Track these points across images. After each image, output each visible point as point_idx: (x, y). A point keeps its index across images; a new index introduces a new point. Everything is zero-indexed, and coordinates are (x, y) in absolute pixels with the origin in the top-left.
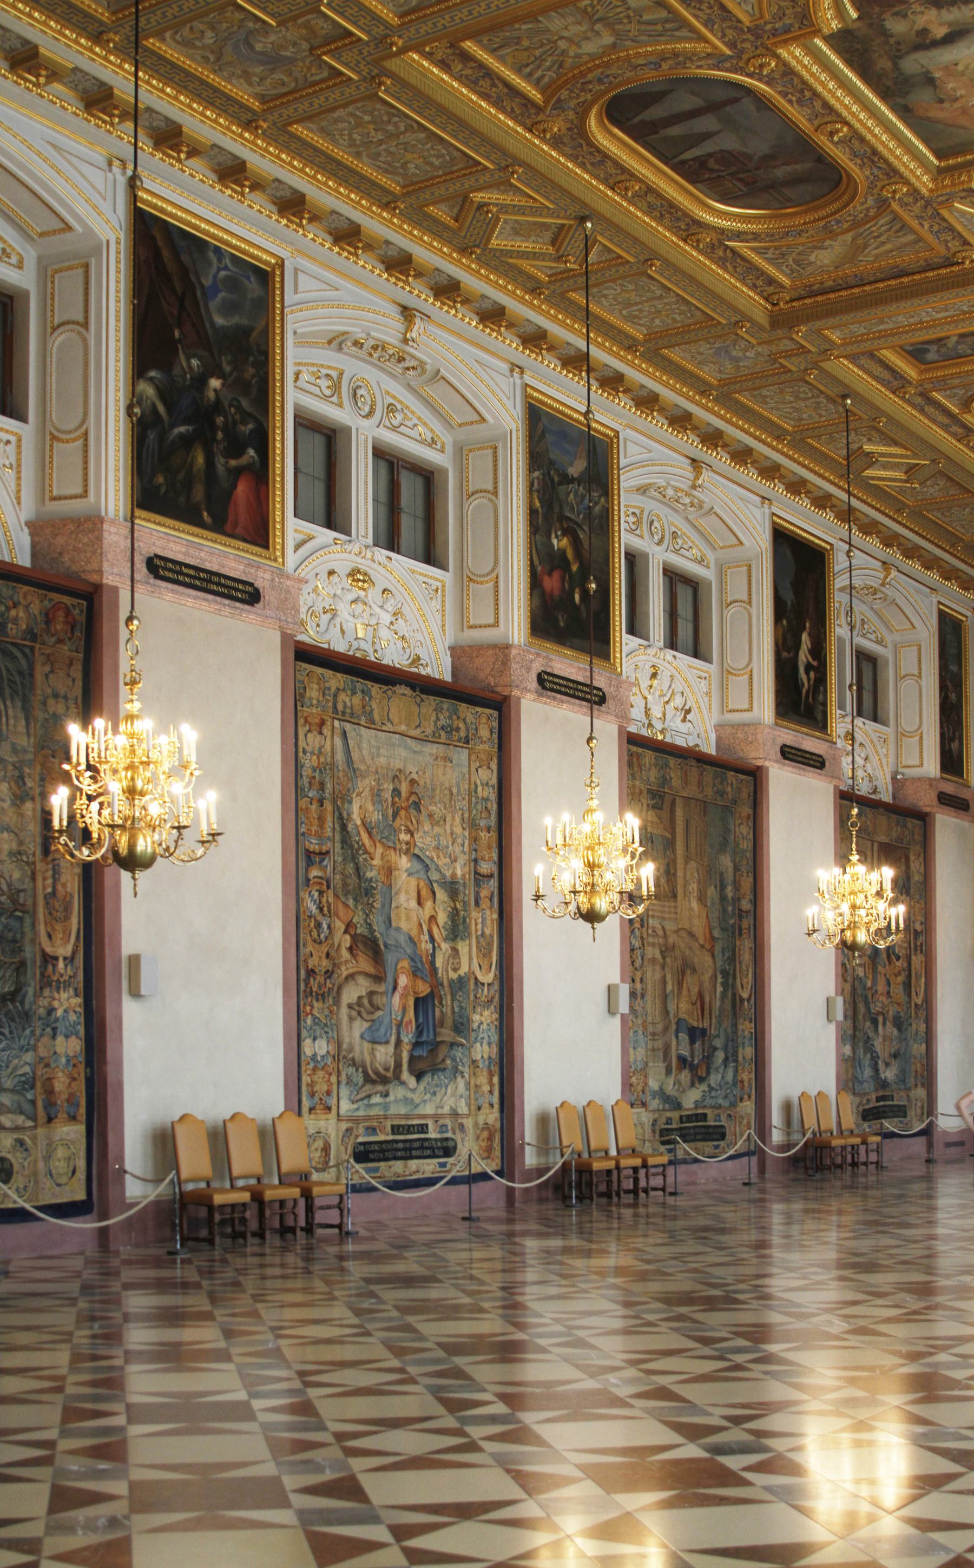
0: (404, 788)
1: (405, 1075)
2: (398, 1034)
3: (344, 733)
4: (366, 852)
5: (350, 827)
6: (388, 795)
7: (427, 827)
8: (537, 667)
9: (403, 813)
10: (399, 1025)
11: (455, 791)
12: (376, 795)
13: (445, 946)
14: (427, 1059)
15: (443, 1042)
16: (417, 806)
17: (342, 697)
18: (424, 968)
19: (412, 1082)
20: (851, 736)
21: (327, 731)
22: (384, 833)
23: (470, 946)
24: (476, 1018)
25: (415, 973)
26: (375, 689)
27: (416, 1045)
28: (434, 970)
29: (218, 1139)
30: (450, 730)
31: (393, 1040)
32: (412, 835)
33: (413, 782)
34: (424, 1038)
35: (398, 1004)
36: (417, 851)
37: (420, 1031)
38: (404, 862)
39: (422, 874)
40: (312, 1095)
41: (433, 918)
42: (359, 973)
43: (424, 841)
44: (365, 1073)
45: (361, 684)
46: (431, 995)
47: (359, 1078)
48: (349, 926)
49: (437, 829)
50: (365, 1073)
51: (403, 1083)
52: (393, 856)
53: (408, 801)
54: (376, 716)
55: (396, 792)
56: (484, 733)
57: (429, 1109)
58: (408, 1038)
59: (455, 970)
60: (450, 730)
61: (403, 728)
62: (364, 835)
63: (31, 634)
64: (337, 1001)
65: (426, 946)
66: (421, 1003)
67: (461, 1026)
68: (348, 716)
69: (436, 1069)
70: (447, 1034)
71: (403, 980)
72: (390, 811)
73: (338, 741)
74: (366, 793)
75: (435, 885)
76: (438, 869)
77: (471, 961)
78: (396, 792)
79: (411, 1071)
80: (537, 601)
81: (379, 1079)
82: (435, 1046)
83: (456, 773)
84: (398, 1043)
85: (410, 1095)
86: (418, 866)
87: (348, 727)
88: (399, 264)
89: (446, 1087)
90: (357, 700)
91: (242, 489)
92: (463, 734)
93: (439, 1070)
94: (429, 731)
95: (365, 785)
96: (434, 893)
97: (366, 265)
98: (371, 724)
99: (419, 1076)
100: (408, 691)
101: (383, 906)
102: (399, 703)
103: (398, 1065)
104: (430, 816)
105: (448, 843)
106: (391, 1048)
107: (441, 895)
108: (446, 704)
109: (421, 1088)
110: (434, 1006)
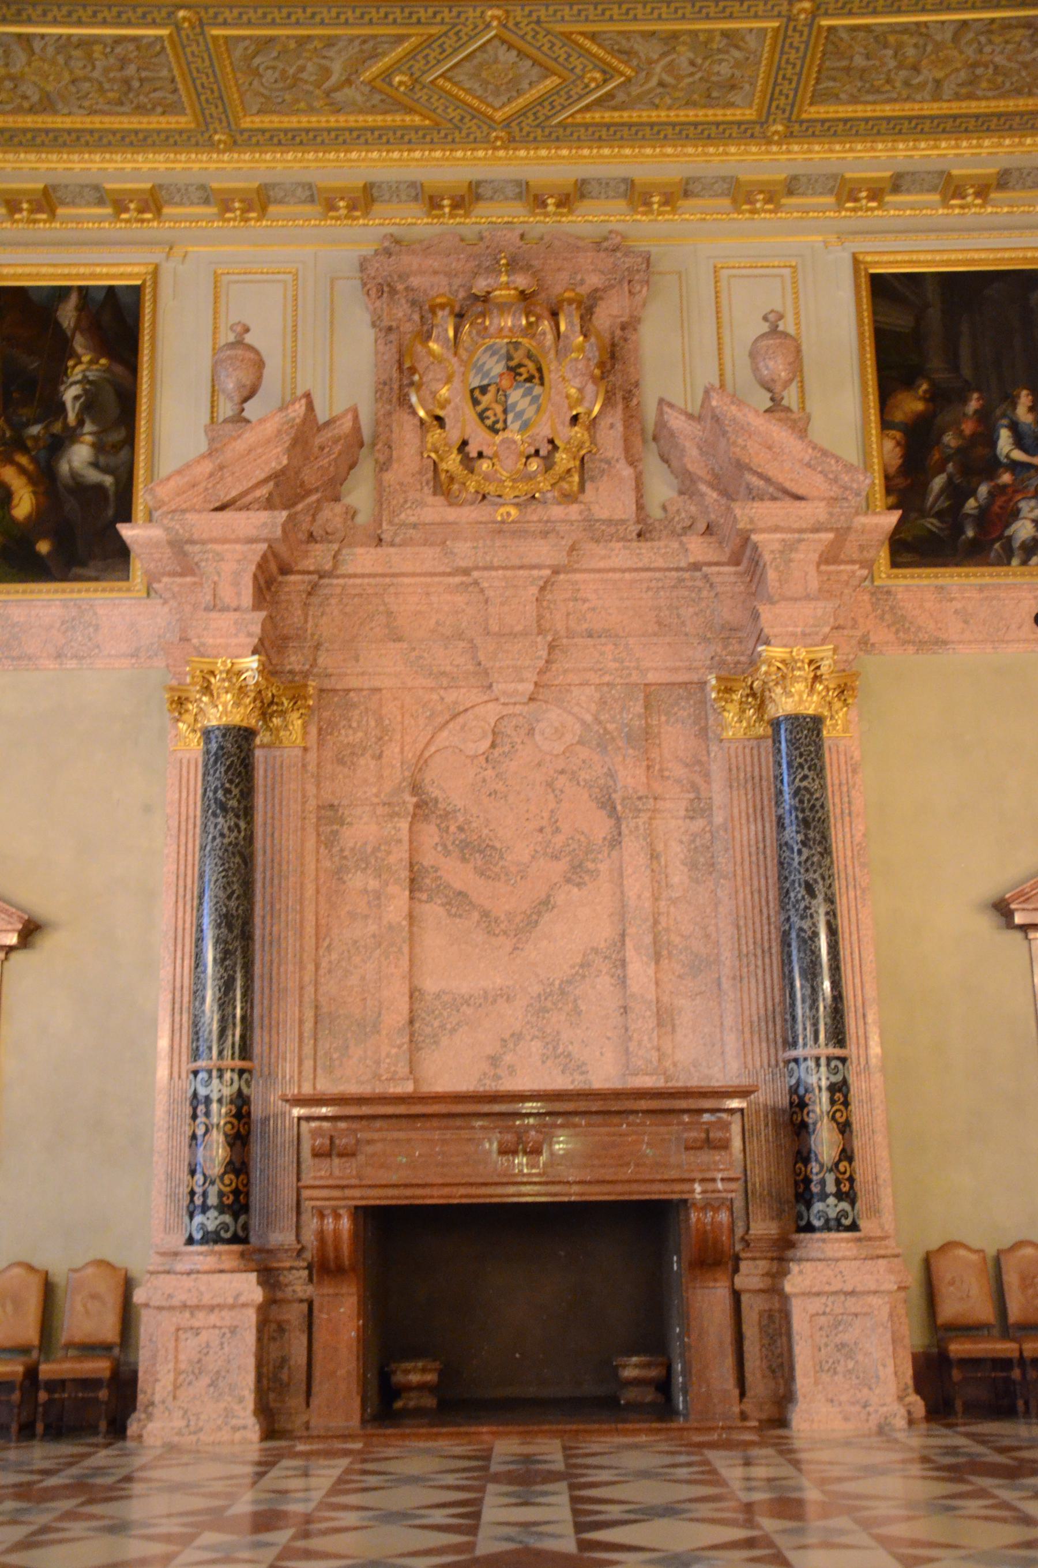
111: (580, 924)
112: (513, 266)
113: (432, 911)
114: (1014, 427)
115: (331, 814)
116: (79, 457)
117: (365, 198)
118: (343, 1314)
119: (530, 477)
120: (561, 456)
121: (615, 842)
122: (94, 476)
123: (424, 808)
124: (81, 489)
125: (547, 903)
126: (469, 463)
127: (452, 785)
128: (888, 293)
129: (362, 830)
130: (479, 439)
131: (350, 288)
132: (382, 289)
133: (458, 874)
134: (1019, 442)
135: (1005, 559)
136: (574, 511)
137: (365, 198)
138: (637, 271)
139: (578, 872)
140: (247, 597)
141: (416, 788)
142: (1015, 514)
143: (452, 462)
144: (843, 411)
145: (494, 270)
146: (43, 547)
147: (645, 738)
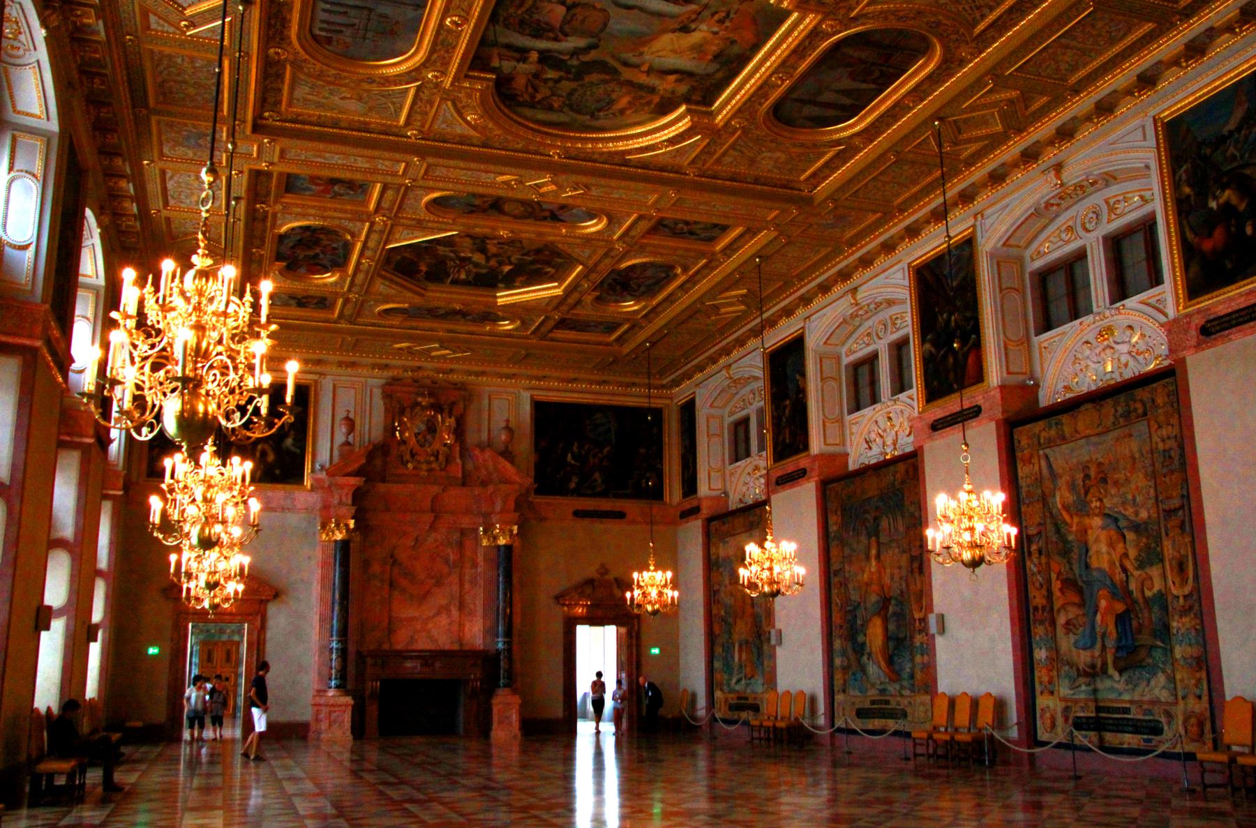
0: (1092, 473)
1: (1111, 671)
2: (1103, 641)
3: (1047, 457)
4: (1067, 524)
5: (1054, 511)
6: (1080, 482)
7: (1113, 491)
8: (1198, 321)
9: (1092, 490)
10: (1104, 635)
11: (1137, 455)
12: (1072, 487)
13: (1136, 573)
14: (1130, 658)
15: (1143, 646)
16: (1104, 480)
17: (1043, 434)
18: (1121, 592)
19: (1116, 675)
20: (757, 468)
21: (1035, 460)
22: (1081, 508)
23: (1164, 568)
24: (1175, 624)
25: (1114, 596)
26: (1065, 418)
27: (1118, 648)
28: (1130, 593)
29: (975, 703)
30: (1127, 415)
31: (1098, 646)
32: (1101, 500)
33: (1100, 464)
34: (1124, 642)
35: (1105, 622)
36: (1107, 511)
37: (1119, 639)
38: (1097, 521)
39: (1113, 526)
40: (1041, 683)
41: (1126, 555)
42: (1068, 604)
44: (1078, 670)
45: (1053, 420)
46: (1127, 611)
47: (1074, 673)
48: (1059, 574)
49: (1122, 490)
50: (1078, 670)
51: (1111, 677)
52: (1087, 521)
54: (1067, 434)
55: (1087, 477)
57: (1126, 697)
58: (1111, 643)
59: (1150, 589)
61: (1088, 432)
62: (1064, 513)
63: (903, 482)
64: (1053, 623)
65: (1119, 576)
66: (1122, 620)
67: (1164, 632)
68: (1050, 443)
69: (1139, 665)
70: (1145, 639)
71: (1103, 603)
72: (1082, 492)
73: (1043, 463)
74: (1064, 487)
75: (1126, 532)
76: (1126, 517)
77: (1157, 580)
78: (1087, 477)
79: (1116, 668)
80: (1194, 268)
81: (1093, 673)
82: (1134, 650)
83: (1132, 444)
84: (1104, 648)
85: (1116, 686)
86: (1109, 521)
87: (1048, 451)
88: (1030, 156)
89: (1149, 681)
90: (1053, 432)
91: (970, 360)
92: (1140, 411)
93: (1140, 666)
94: (1109, 423)
95: (1062, 482)
96: (1124, 536)
97: (1018, 176)
98: (1064, 439)
99: (1121, 672)
100: (1089, 406)
101: (1080, 556)
103: (1104, 664)
104: (1116, 483)
105: (1136, 496)
106: (1097, 653)
107: (1130, 536)
108: (1122, 398)
109: (1125, 676)
110: (1130, 619)
111: (439, 598)
112: (431, 395)
113: (396, 593)
114: (573, 453)
115: (366, 564)
116: (289, 442)
117: (386, 367)
118: (373, 711)
119: (429, 463)
120: (441, 457)
121: (450, 574)
122: (293, 449)
123: (395, 562)
124: (288, 452)
125: (428, 593)
126: (413, 455)
127: (402, 556)
128: (540, 408)
129: (376, 568)
130: (417, 448)
131: (378, 393)
132: (387, 396)
133: (404, 583)
134: (573, 458)
135: (566, 495)
136: (443, 473)
137: (387, 366)
138: (466, 393)
139: (439, 583)
140: (350, 502)
141: (392, 556)
142: (570, 481)
143: (408, 457)
144: (524, 446)
145: (423, 395)
146: (277, 472)
147: (461, 544)
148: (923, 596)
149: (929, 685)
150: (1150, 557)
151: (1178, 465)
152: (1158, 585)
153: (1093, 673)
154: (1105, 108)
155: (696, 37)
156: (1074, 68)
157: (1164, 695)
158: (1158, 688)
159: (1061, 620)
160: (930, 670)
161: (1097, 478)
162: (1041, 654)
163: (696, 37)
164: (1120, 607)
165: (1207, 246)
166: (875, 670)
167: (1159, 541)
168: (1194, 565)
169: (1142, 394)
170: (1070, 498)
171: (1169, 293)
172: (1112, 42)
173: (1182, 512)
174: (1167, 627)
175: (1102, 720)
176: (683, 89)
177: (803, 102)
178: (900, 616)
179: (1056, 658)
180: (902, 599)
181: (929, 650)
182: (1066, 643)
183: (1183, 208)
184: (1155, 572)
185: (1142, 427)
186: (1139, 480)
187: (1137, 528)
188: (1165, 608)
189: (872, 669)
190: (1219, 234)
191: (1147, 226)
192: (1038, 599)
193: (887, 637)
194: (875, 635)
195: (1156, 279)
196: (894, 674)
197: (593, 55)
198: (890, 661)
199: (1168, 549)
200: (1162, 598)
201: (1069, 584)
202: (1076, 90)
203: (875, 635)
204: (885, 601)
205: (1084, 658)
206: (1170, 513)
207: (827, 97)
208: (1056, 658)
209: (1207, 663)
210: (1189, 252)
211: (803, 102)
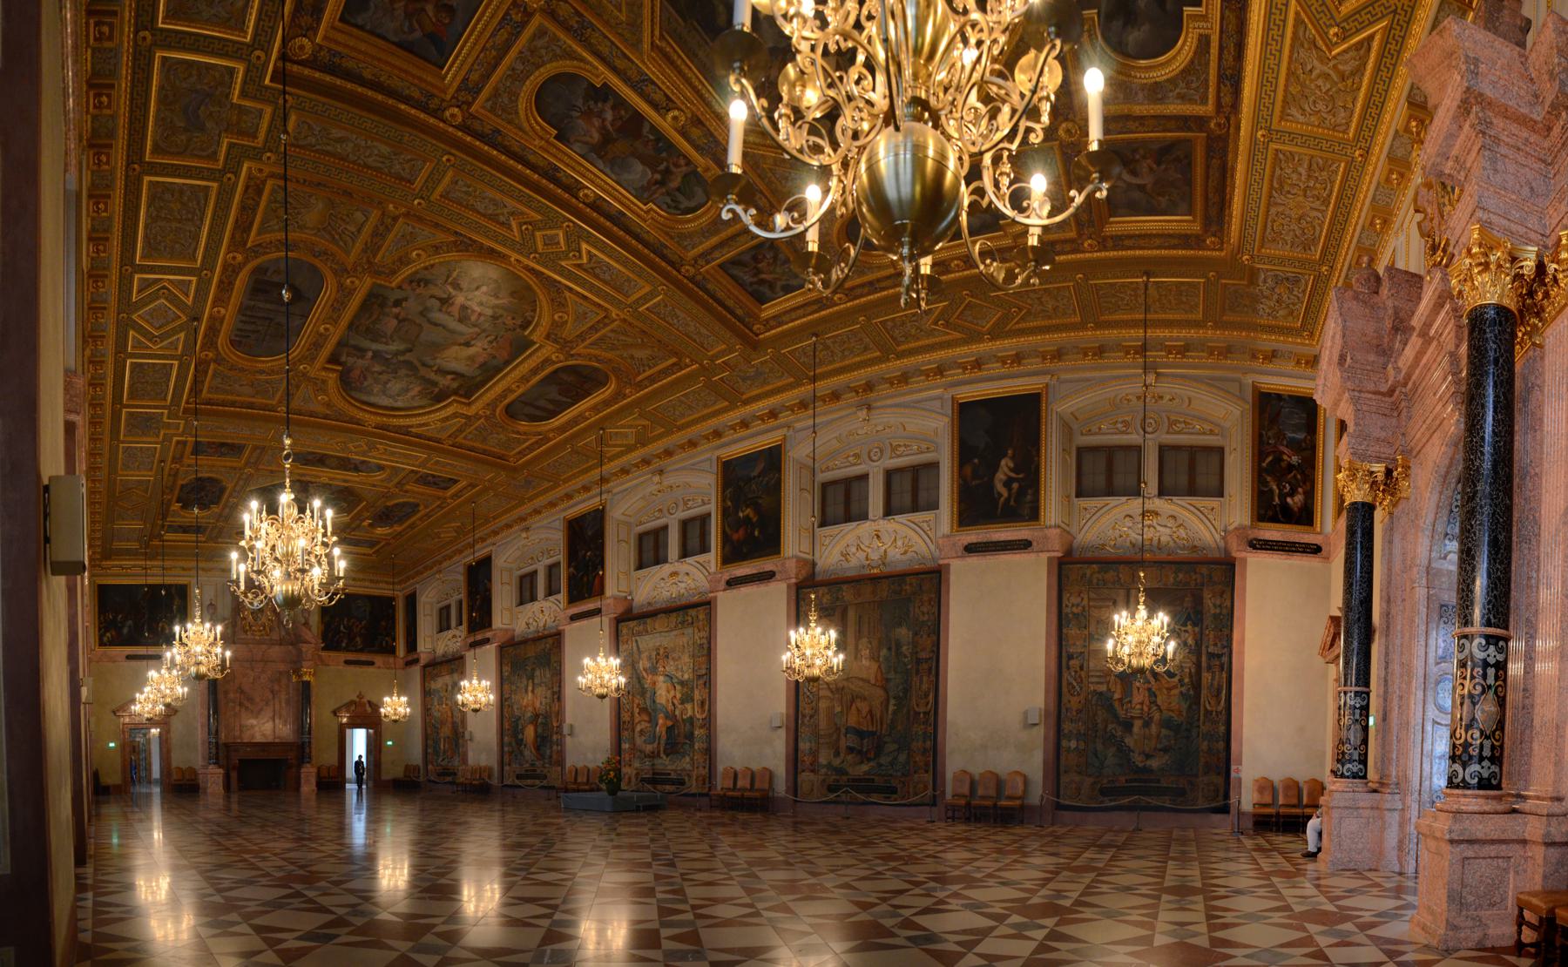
12: (650, 658)
22: (653, 670)
25: (667, 717)
30: (683, 623)
38: (661, 678)
43: (670, 669)
53: (663, 655)
56: (701, 616)
60: (683, 623)
65: (670, 707)
66: (670, 729)
67: (690, 736)
77: (689, 710)
95: (644, 655)
102: (659, 623)
105: (683, 667)
148: (560, 713)
149: (561, 762)
150: (687, 698)
151: (707, 652)
152: (690, 713)
153: (654, 755)
154: (692, 444)
155: (471, 351)
156: (682, 415)
157: (688, 767)
158: (685, 763)
159: (638, 728)
160: (561, 753)
161: (663, 655)
162: (626, 746)
163: (471, 351)
164: (670, 723)
165: (735, 537)
166: (529, 753)
167: (692, 689)
168: (709, 704)
169: (692, 612)
170: (648, 665)
171: (712, 558)
172: (706, 406)
173: (707, 677)
174: (692, 734)
175: (656, 779)
176: (455, 385)
177: (526, 404)
178: (545, 725)
179: (634, 748)
180: (547, 716)
181: (561, 743)
182: (639, 741)
183: (725, 513)
184: (689, 706)
185: (690, 630)
186: (686, 658)
187: (682, 683)
188: (692, 724)
189: (527, 753)
190: (741, 532)
191: (704, 519)
192: (626, 717)
193: (536, 736)
194: (530, 733)
195: (704, 549)
196: (541, 756)
197: (408, 357)
198: (538, 748)
199: (697, 695)
200: (691, 720)
201: (643, 710)
202: (680, 428)
203: (530, 733)
204: (537, 716)
205: (649, 748)
206: (700, 677)
207: (542, 403)
208: (634, 748)
209: (710, 752)
210: (726, 538)
211: (526, 404)
